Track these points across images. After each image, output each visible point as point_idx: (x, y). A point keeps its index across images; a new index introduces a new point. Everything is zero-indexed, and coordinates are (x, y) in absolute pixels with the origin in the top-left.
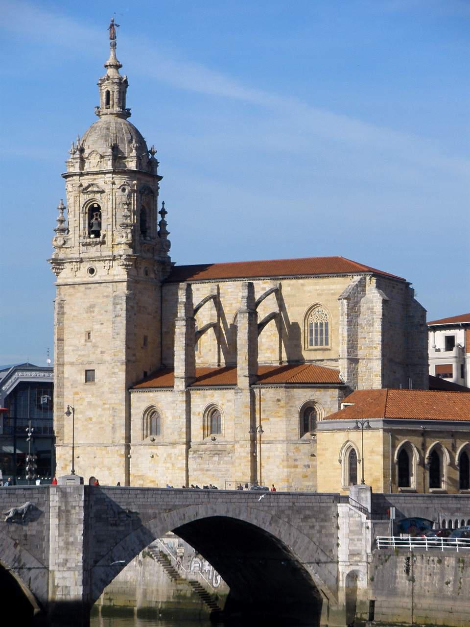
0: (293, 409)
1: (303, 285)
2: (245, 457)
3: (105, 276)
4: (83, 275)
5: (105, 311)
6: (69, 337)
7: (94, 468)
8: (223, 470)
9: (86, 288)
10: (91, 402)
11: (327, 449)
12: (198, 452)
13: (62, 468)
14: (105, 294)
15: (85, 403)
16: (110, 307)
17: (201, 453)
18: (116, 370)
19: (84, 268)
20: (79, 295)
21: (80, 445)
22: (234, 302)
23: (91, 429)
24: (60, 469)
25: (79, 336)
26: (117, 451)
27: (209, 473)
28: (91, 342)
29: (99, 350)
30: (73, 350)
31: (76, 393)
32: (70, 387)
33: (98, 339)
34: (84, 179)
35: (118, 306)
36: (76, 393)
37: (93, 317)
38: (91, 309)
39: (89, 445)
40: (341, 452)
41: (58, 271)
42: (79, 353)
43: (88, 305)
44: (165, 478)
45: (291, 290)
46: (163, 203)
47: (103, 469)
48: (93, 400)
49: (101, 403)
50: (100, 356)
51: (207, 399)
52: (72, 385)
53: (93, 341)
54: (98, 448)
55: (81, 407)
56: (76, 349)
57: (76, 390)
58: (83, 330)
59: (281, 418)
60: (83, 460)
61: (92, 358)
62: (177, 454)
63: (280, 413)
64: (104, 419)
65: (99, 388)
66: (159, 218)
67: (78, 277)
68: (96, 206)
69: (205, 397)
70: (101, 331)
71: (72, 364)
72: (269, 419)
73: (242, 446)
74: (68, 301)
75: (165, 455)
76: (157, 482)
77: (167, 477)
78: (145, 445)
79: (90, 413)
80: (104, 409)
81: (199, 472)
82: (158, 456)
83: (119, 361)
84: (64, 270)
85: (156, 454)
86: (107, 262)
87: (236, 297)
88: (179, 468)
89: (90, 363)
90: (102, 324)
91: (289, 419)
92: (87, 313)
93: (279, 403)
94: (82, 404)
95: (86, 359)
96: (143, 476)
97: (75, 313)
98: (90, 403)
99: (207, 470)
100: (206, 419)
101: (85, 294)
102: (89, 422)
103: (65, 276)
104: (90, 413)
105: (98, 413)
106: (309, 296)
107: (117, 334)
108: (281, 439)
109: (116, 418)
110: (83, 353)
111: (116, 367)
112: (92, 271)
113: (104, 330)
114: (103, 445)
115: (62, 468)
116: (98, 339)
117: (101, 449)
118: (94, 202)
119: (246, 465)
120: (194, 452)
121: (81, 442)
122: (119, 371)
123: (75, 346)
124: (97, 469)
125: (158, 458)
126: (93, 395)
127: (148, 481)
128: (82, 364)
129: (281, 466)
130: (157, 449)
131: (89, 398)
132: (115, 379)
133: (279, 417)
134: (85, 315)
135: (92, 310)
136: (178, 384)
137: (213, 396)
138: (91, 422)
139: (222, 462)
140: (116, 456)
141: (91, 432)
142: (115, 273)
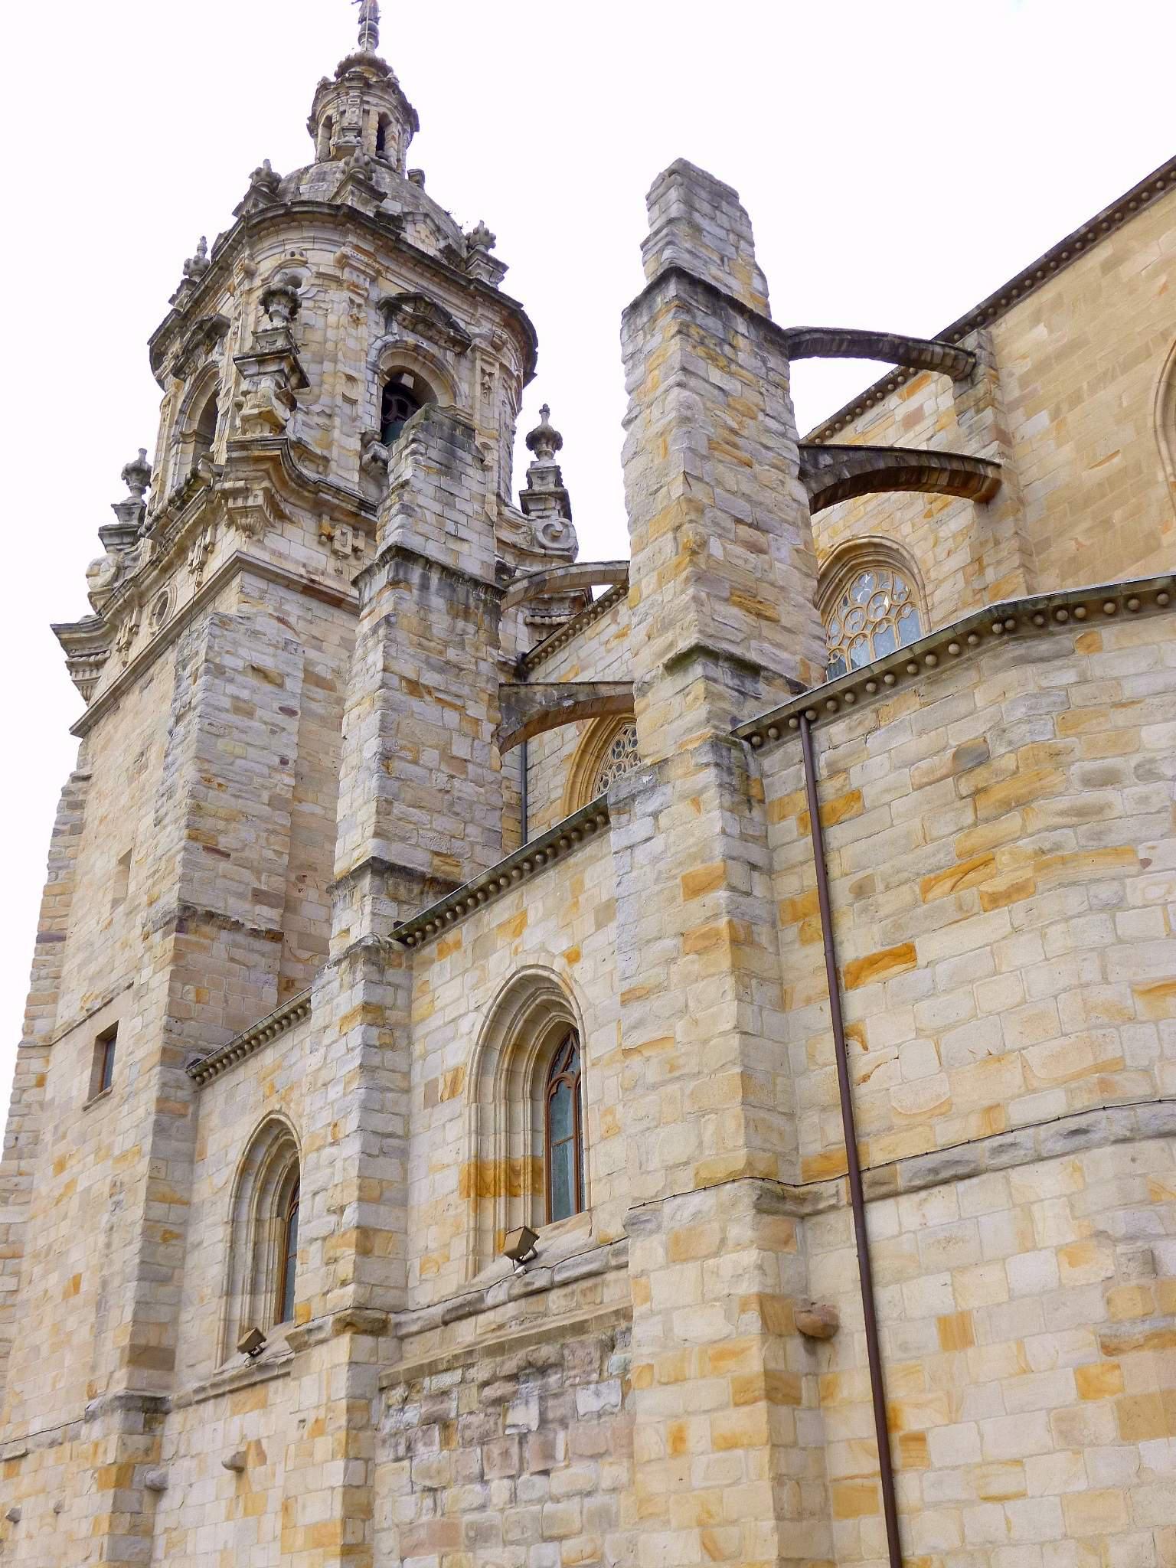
0: (1119, 799)
1: (1108, 266)
2: (720, 1353)
9: (142, 689)
12: (427, 1382)
41: (87, 676)
45: (1051, 331)
46: (545, 411)
51: (493, 960)
59: (1020, 906)
62: (311, 1417)
63: (1003, 858)
66: (523, 458)
69: (482, 948)
72: (906, 954)
73: (680, 1252)
91: (1105, 892)
93: (981, 776)
100: (496, 1115)
106: (1165, 287)
108: (1054, 1103)
119: (728, 1443)
120: (410, 1386)
129: (1101, 1418)
133: (995, 900)
139: (561, 1438)
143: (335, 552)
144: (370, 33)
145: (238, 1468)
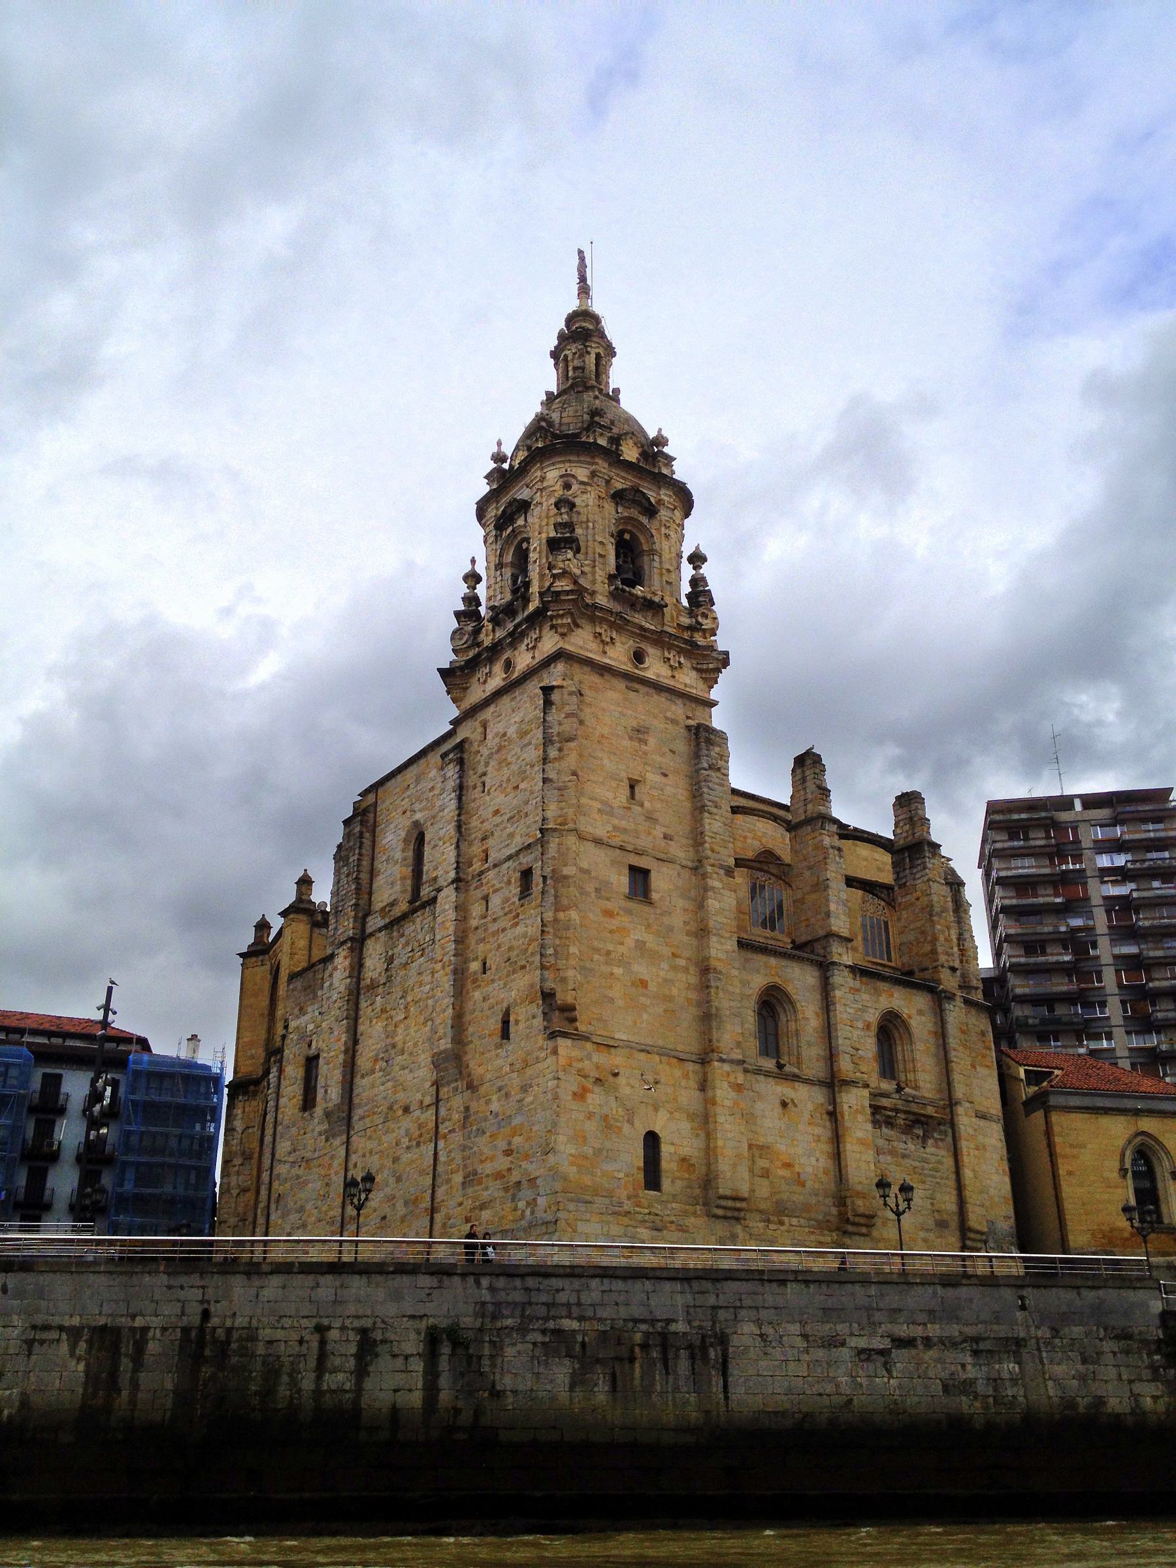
3: (664, 677)
4: (618, 655)
5: (670, 750)
6: (592, 778)
7: (656, 1109)
8: (933, 1159)
10: (644, 943)
11: (1082, 1146)
13: (575, 1094)
14: (669, 714)
15: (630, 942)
16: (682, 746)
17: (890, 1113)
18: (717, 884)
19: (623, 644)
20: (611, 694)
21: (621, 1044)
22: (749, 835)
23: (644, 1008)
24: (570, 1098)
25: (614, 784)
26: (728, 1075)
27: (908, 1162)
28: (642, 805)
29: (659, 831)
30: (600, 811)
31: (609, 914)
32: (593, 895)
33: (658, 806)
34: (618, 475)
35: (717, 749)
36: (609, 914)
37: (646, 753)
38: (639, 733)
39: (639, 1047)
40: (1123, 1155)
42: (616, 822)
43: (635, 724)
44: (813, 1160)
47: (677, 1115)
48: (650, 939)
49: (666, 951)
50: (663, 843)
52: (597, 890)
53: (647, 804)
54: (664, 1059)
55: (621, 949)
56: (607, 810)
57: (609, 905)
58: (624, 775)
60: (628, 1084)
61: (643, 842)
62: (855, 1108)
64: (675, 992)
65: (661, 915)
67: (610, 658)
68: (627, 536)
70: (662, 790)
71: (598, 842)
74: (588, 699)
75: (810, 1106)
76: (797, 1169)
77: (817, 1160)
78: (767, 1074)
79: (641, 969)
80: (674, 968)
81: (889, 1158)
82: (796, 1106)
83: (721, 867)
84: (580, 630)
85: (792, 1100)
86: (673, 653)
87: (752, 827)
88: (861, 1142)
89: (638, 853)
90: (665, 775)
92: (631, 738)
93: (984, 1039)
94: (622, 944)
95: (631, 842)
96: (768, 1148)
97: (606, 731)
98: (640, 945)
99: (904, 1156)
101: (626, 699)
102: (641, 990)
103: (581, 643)
104: (641, 969)
105: (662, 973)
107: (716, 807)
109: (721, 994)
110: (624, 824)
111: (715, 876)
112: (639, 657)
113: (669, 790)
114: (672, 1053)
115: (575, 1094)
116: (658, 806)
117: (669, 1064)
118: (629, 528)
121: (624, 1037)
122: (723, 888)
123: (605, 803)
124: (663, 1115)
125: (796, 1109)
126: (648, 926)
127: (779, 1164)
128: (621, 848)
130: (793, 1088)
131: (638, 934)
132: (717, 905)
134: (626, 743)
135: (641, 736)
136: (840, 950)
137: (892, 996)
138: (645, 991)
140: (725, 1085)
141: (645, 1016)
142: (688, 681)
143: (602, 641)
144: (584, 290)
145: (784, 1104)
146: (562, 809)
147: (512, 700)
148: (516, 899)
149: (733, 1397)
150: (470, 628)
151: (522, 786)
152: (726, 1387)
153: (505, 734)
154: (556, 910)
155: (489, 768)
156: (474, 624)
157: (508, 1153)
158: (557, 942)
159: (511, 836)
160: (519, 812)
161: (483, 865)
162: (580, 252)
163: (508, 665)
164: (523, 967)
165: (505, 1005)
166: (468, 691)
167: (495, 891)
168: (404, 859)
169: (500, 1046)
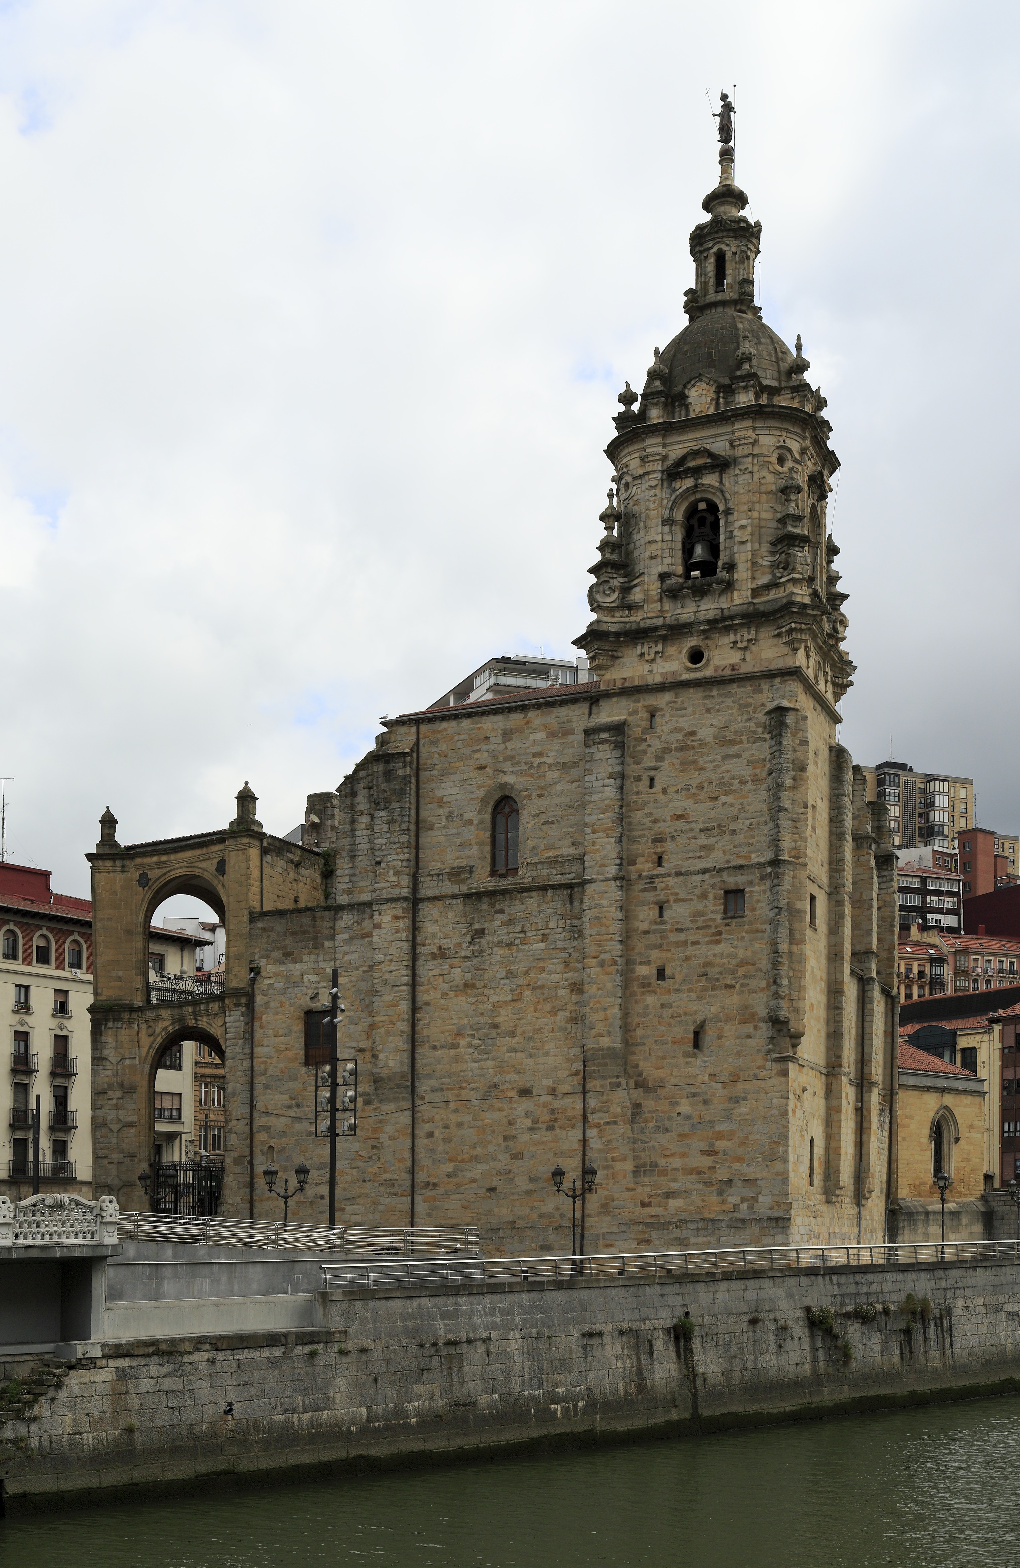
146: (795, 841)
147: (706, 697)
148: (718, 917)
149: (956, 1351)
150: (615, 583)
151: (723, 799)
152: (952, 1345)
153: (693, 733)
154: (791, 943)
155: (665, 764)
156: (621, 580)
157: (711, 1152)
158: (791, 974)
159: (707, 849)
160: (719, 826)
161: (654, 869)
162: (724, 97)
163: (696, 656)
164: (730, 987)
165: (699, 1018)
166: (618, 661)
167: (677, 900)
168: (482, 822)
169: (687, 1055)
